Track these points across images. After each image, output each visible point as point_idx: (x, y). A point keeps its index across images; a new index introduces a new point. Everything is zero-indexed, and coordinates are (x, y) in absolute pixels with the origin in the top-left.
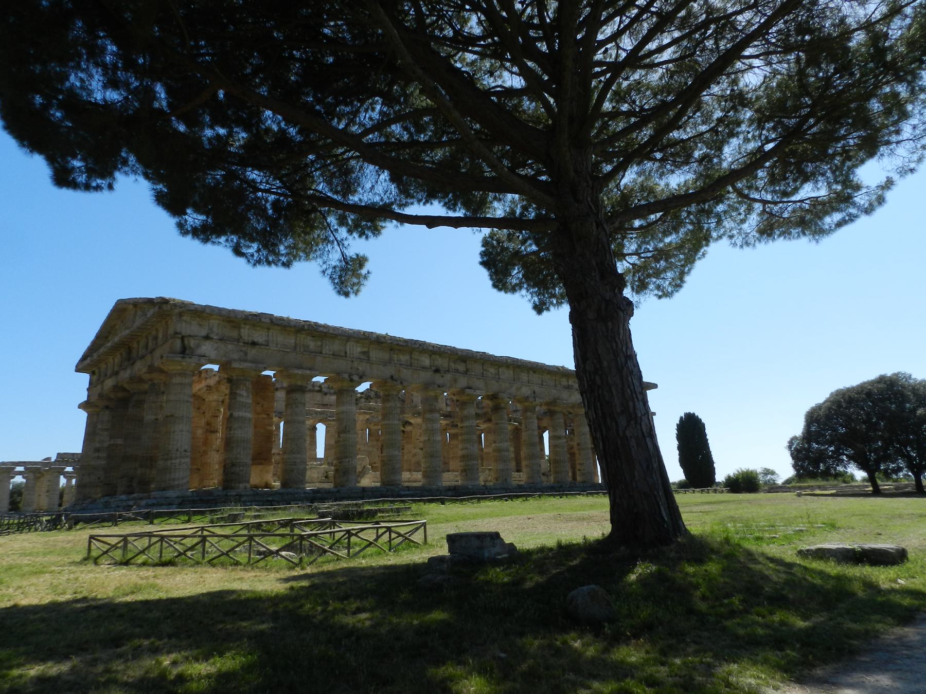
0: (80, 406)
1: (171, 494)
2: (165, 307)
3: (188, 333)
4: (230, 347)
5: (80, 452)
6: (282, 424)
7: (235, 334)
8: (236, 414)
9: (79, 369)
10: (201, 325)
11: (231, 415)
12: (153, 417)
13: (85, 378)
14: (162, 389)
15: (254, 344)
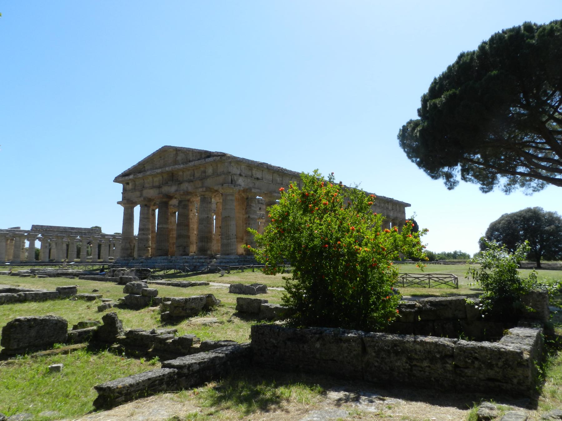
0: (119, 203)
1: (232, 257)
2: (223, 158)
3: (234, 172)
4: (249, 180)
5: (120, 231)
6: (157, 211)
7: (250, 173)
8: (252, 216)
9: (117, 180)
10: (237, 168)
11: (249, 217)
12: (206, 216)
13: (120, 186)
14: (210, 201)
15: (258, 179)
